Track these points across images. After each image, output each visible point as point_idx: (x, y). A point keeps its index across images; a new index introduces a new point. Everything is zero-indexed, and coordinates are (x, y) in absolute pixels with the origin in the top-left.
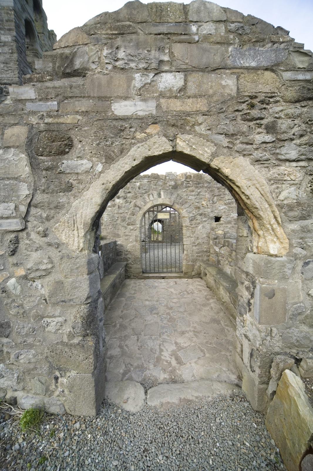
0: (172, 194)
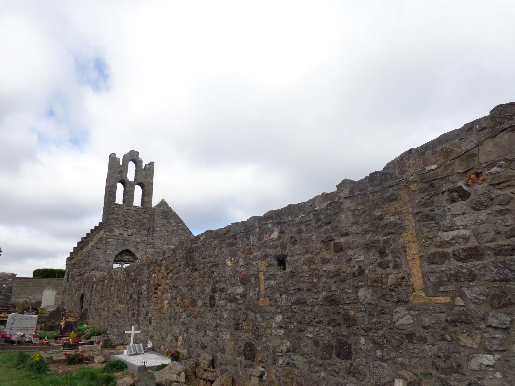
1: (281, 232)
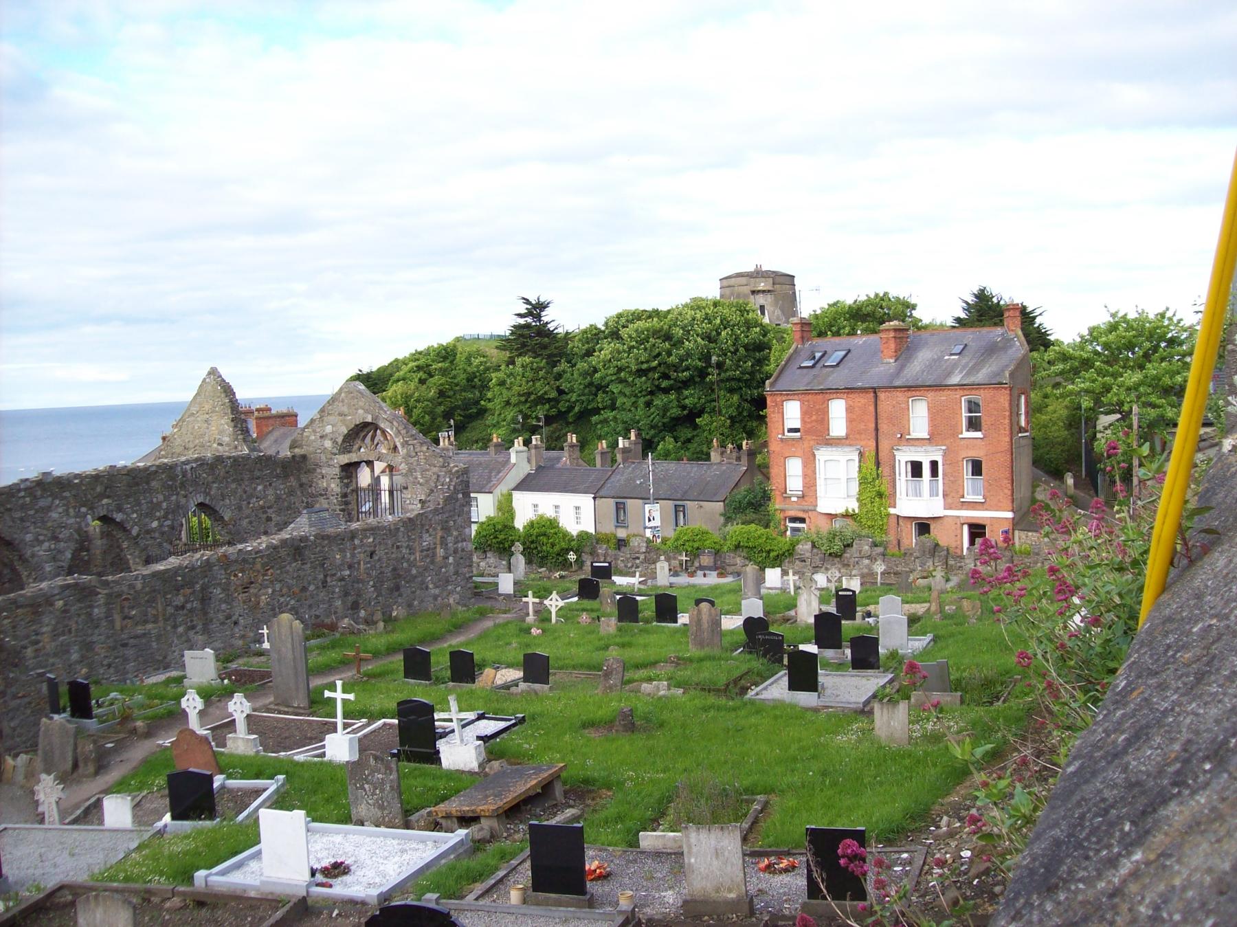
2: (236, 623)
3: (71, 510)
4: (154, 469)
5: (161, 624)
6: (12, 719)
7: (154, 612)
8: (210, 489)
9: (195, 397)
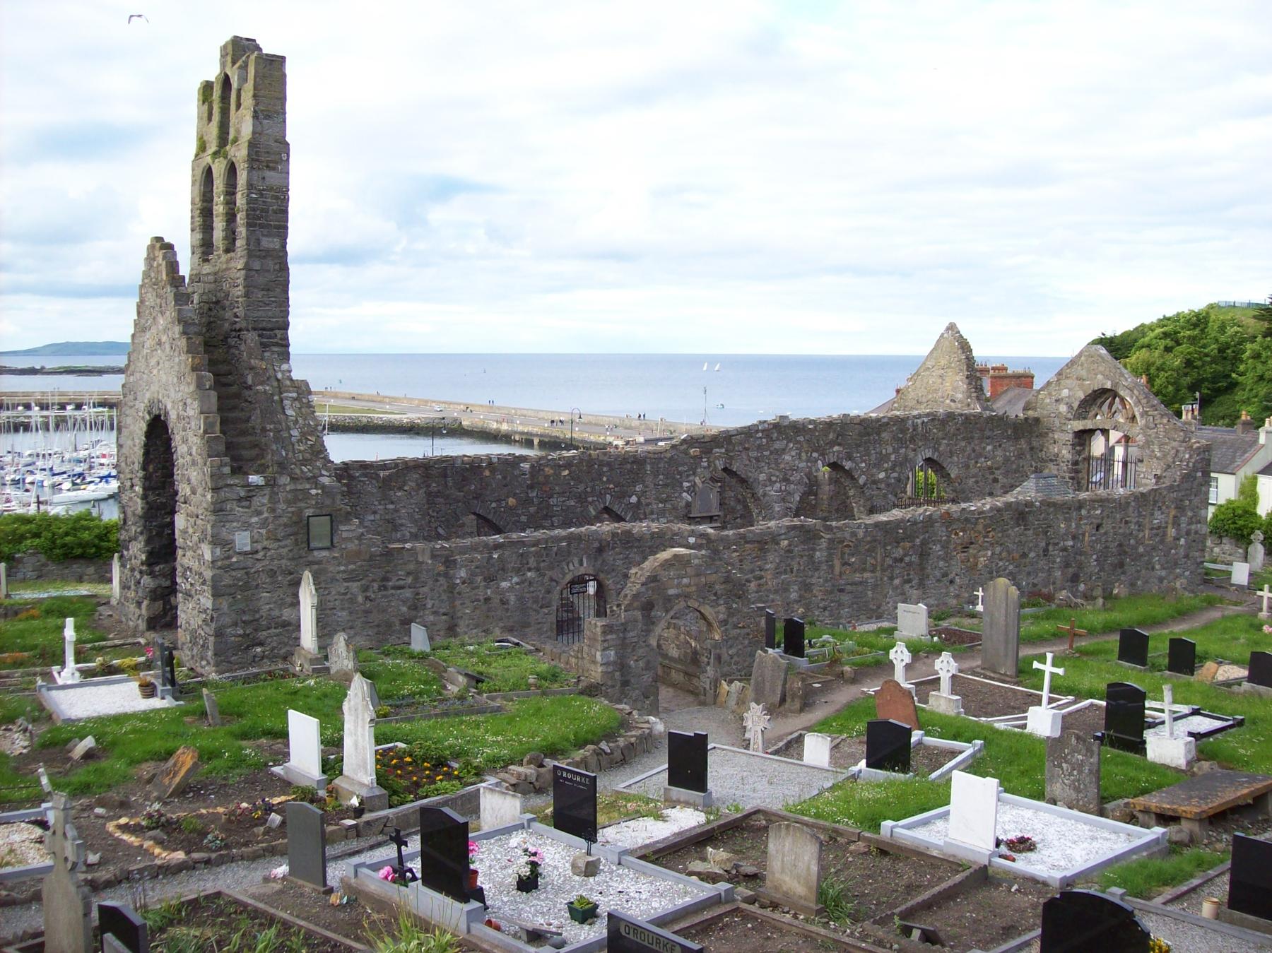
0: (596, 560)
1: (1102, 511)
2: (952, 582)
3: (804, 456)
4: (886, 420)
5: (878, 574)
6: (731, 647)
7: (873, 561)
8: (940, 445)
9: (932, 352)
